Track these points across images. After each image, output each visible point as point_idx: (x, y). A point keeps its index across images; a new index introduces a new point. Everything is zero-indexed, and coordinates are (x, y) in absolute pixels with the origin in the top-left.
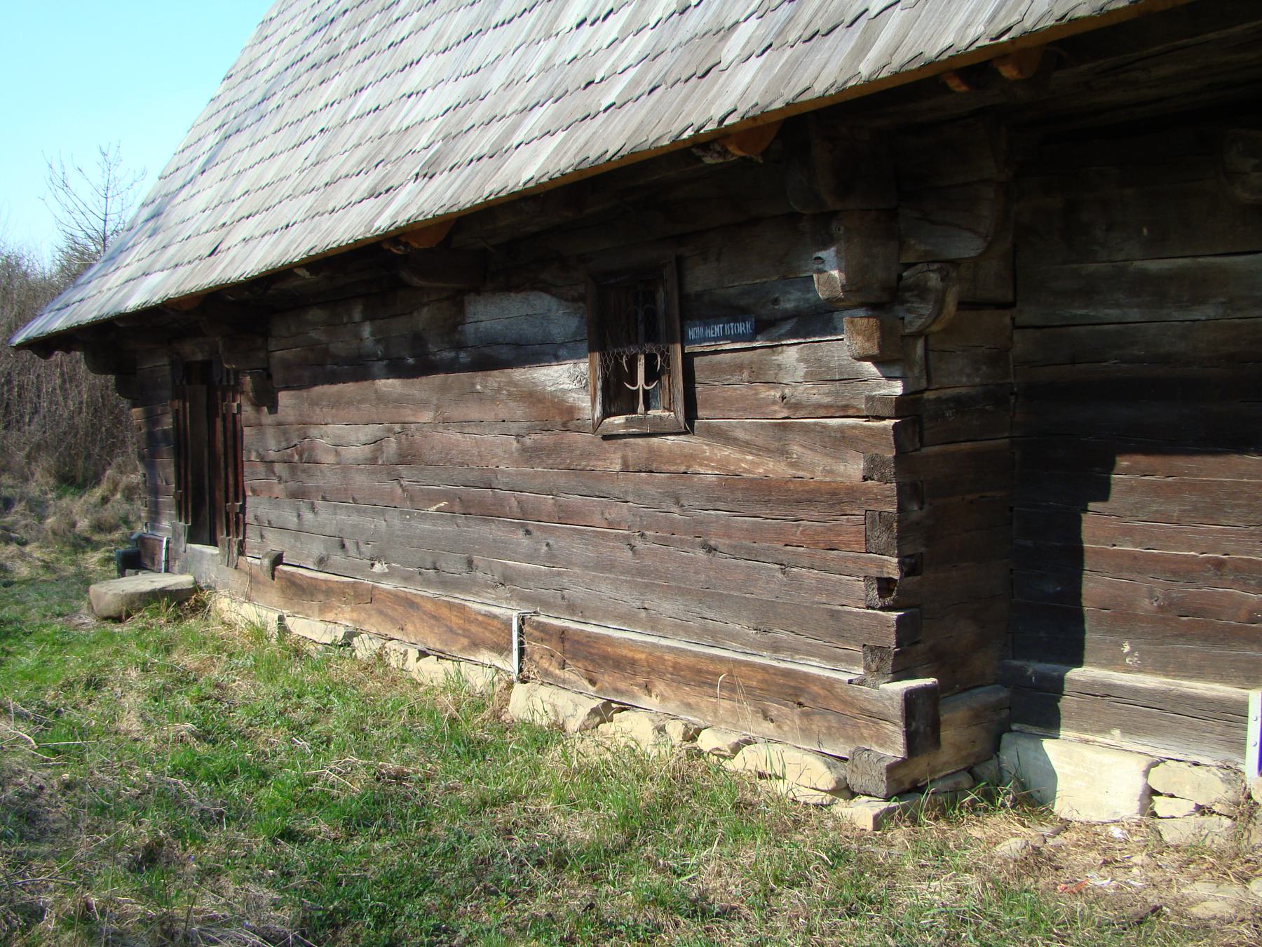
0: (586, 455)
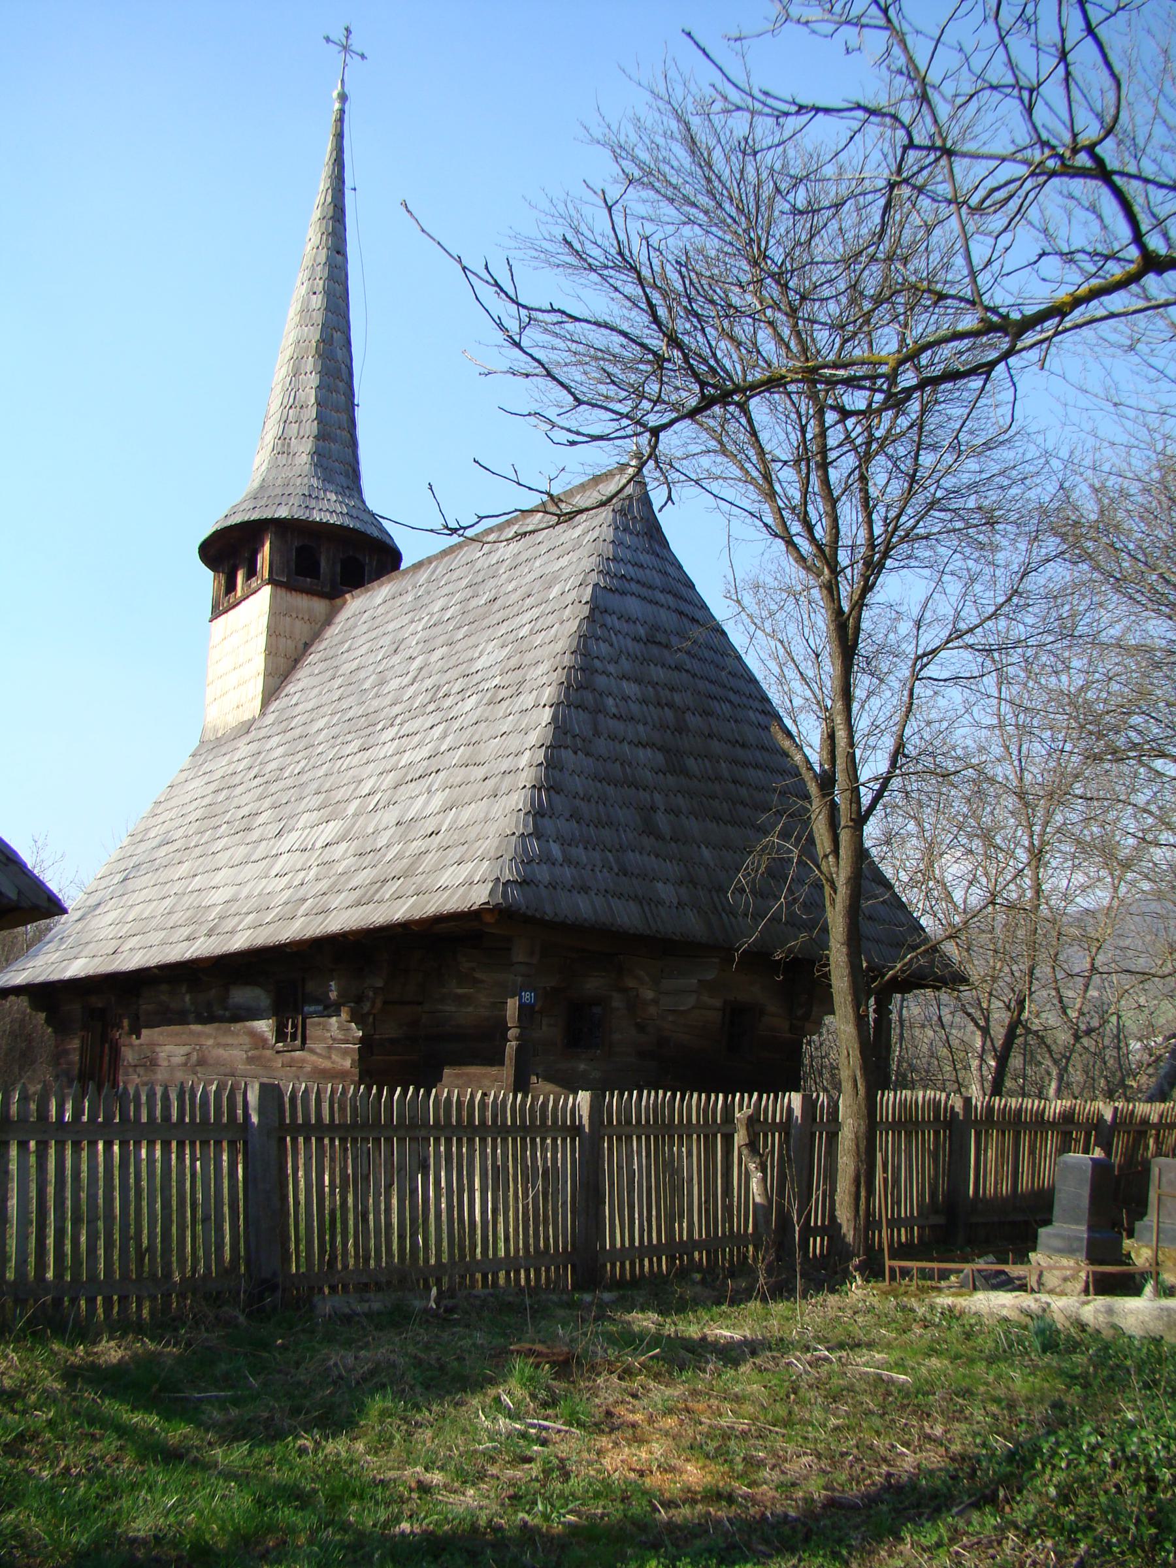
0: (270, 1060)
